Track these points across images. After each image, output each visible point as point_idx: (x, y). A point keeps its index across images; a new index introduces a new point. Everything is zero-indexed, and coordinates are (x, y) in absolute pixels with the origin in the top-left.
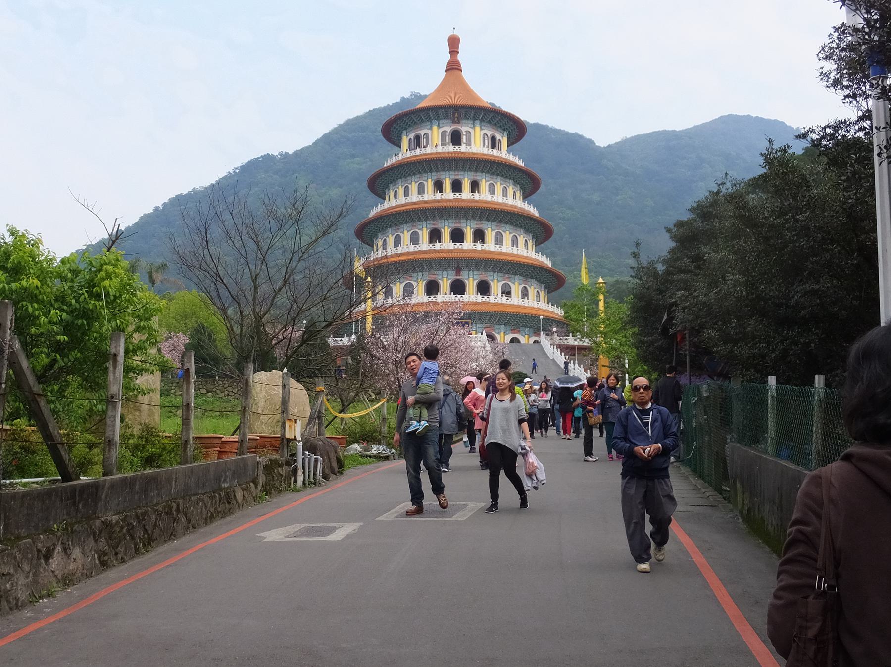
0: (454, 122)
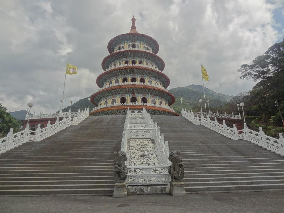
0: (133, 41)
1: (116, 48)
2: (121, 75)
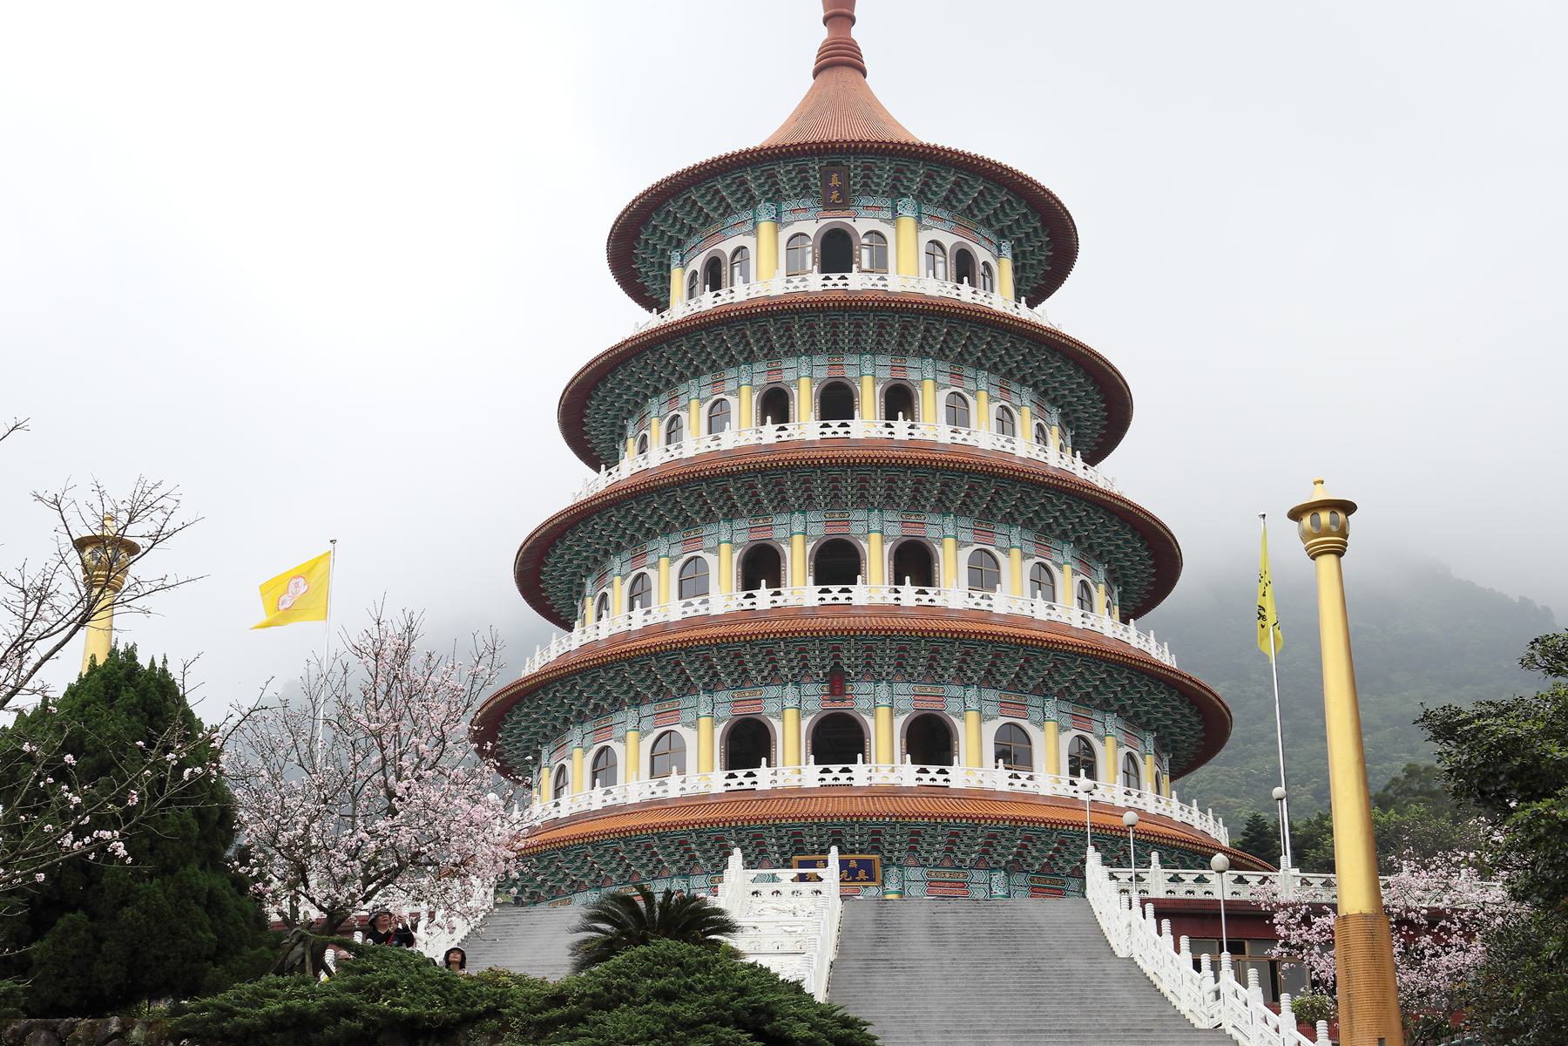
0: (829, 206)
1: (683, 266)
2: (709, 689)
